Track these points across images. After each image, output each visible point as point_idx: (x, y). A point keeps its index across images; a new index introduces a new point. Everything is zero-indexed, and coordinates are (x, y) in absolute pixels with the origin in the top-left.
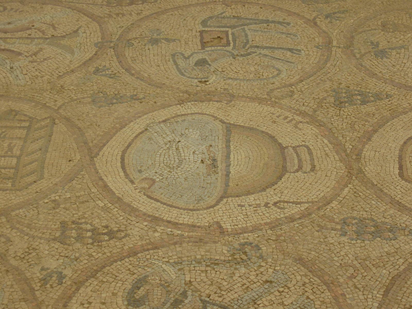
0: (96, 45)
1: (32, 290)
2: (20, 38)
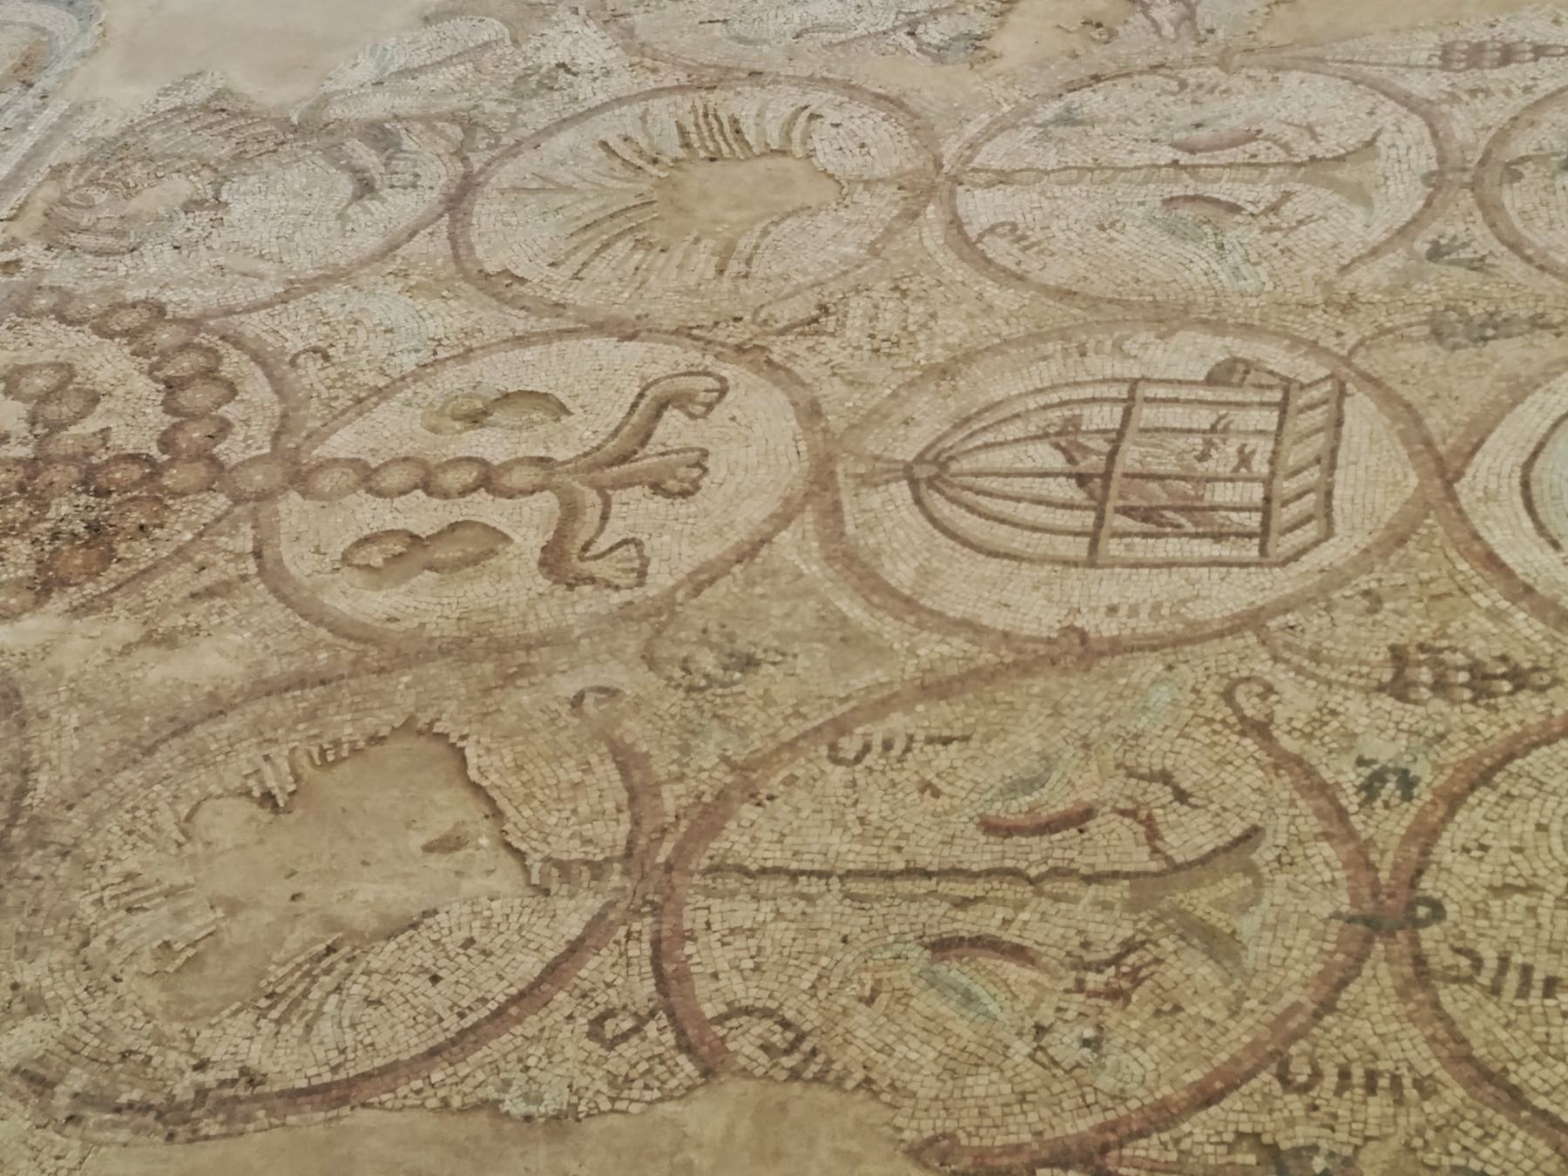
0: (1427, 178)
1: (1343, 814)
2: (1230, 165)
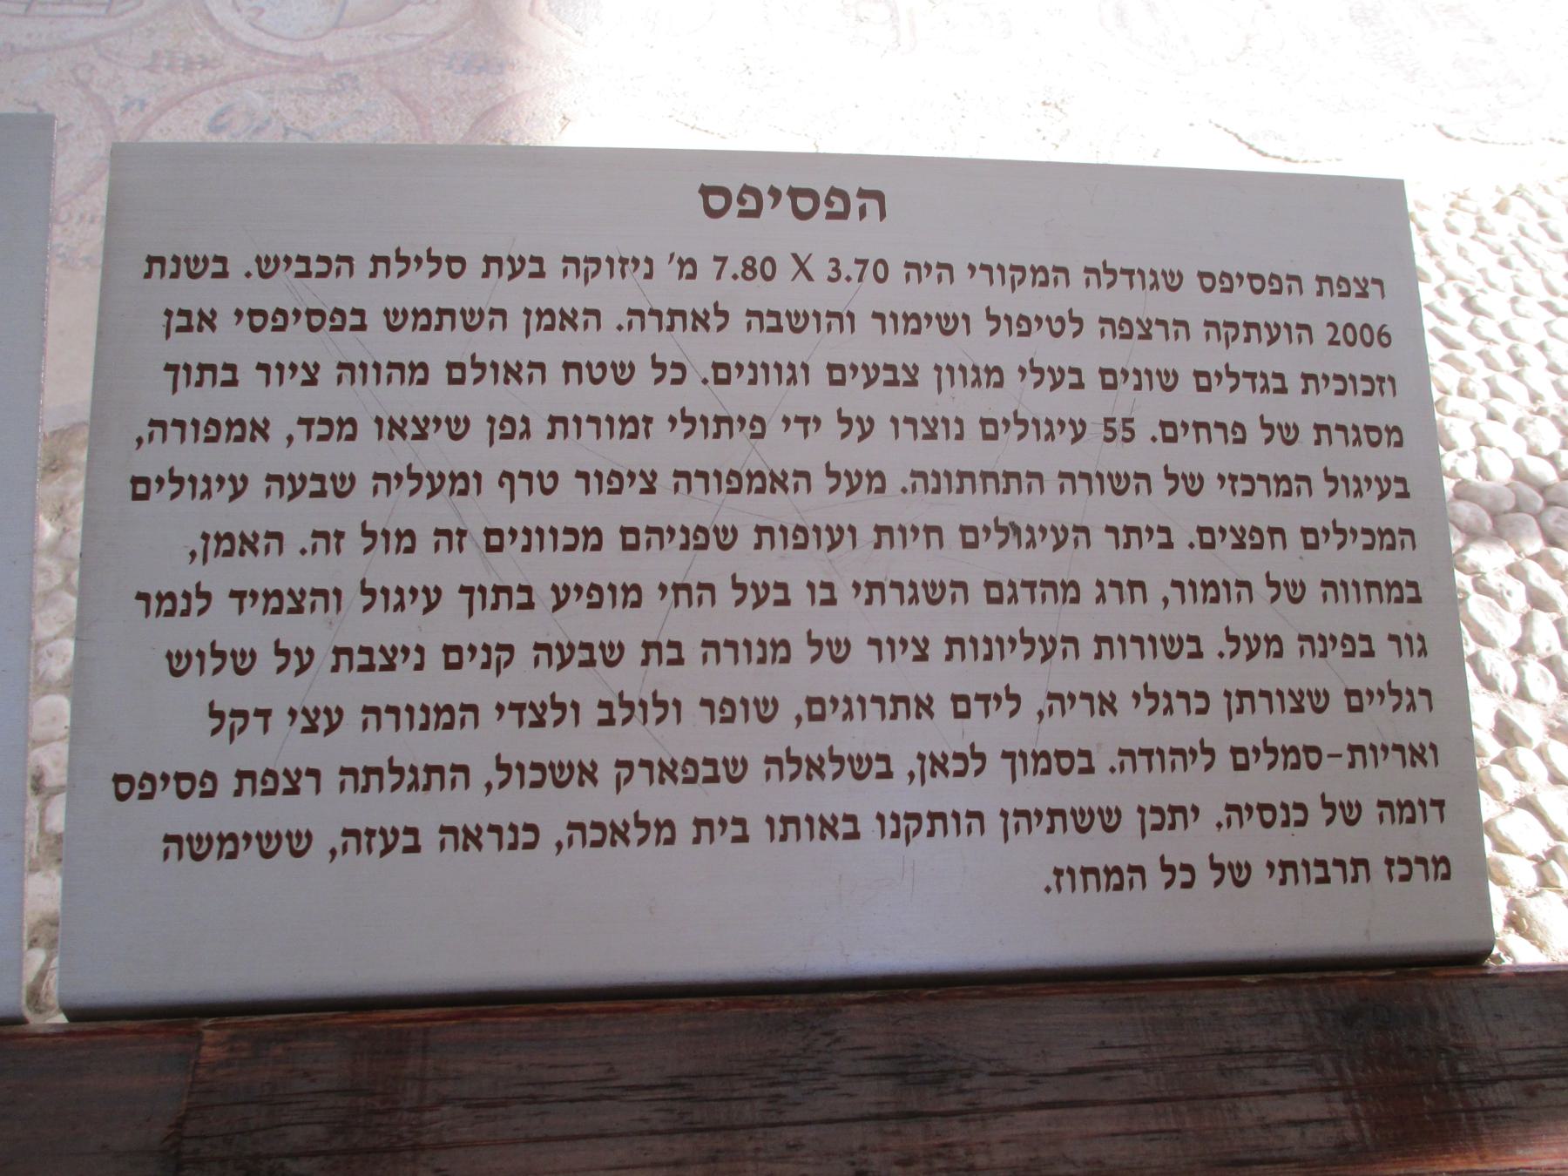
1: (111, 117)
